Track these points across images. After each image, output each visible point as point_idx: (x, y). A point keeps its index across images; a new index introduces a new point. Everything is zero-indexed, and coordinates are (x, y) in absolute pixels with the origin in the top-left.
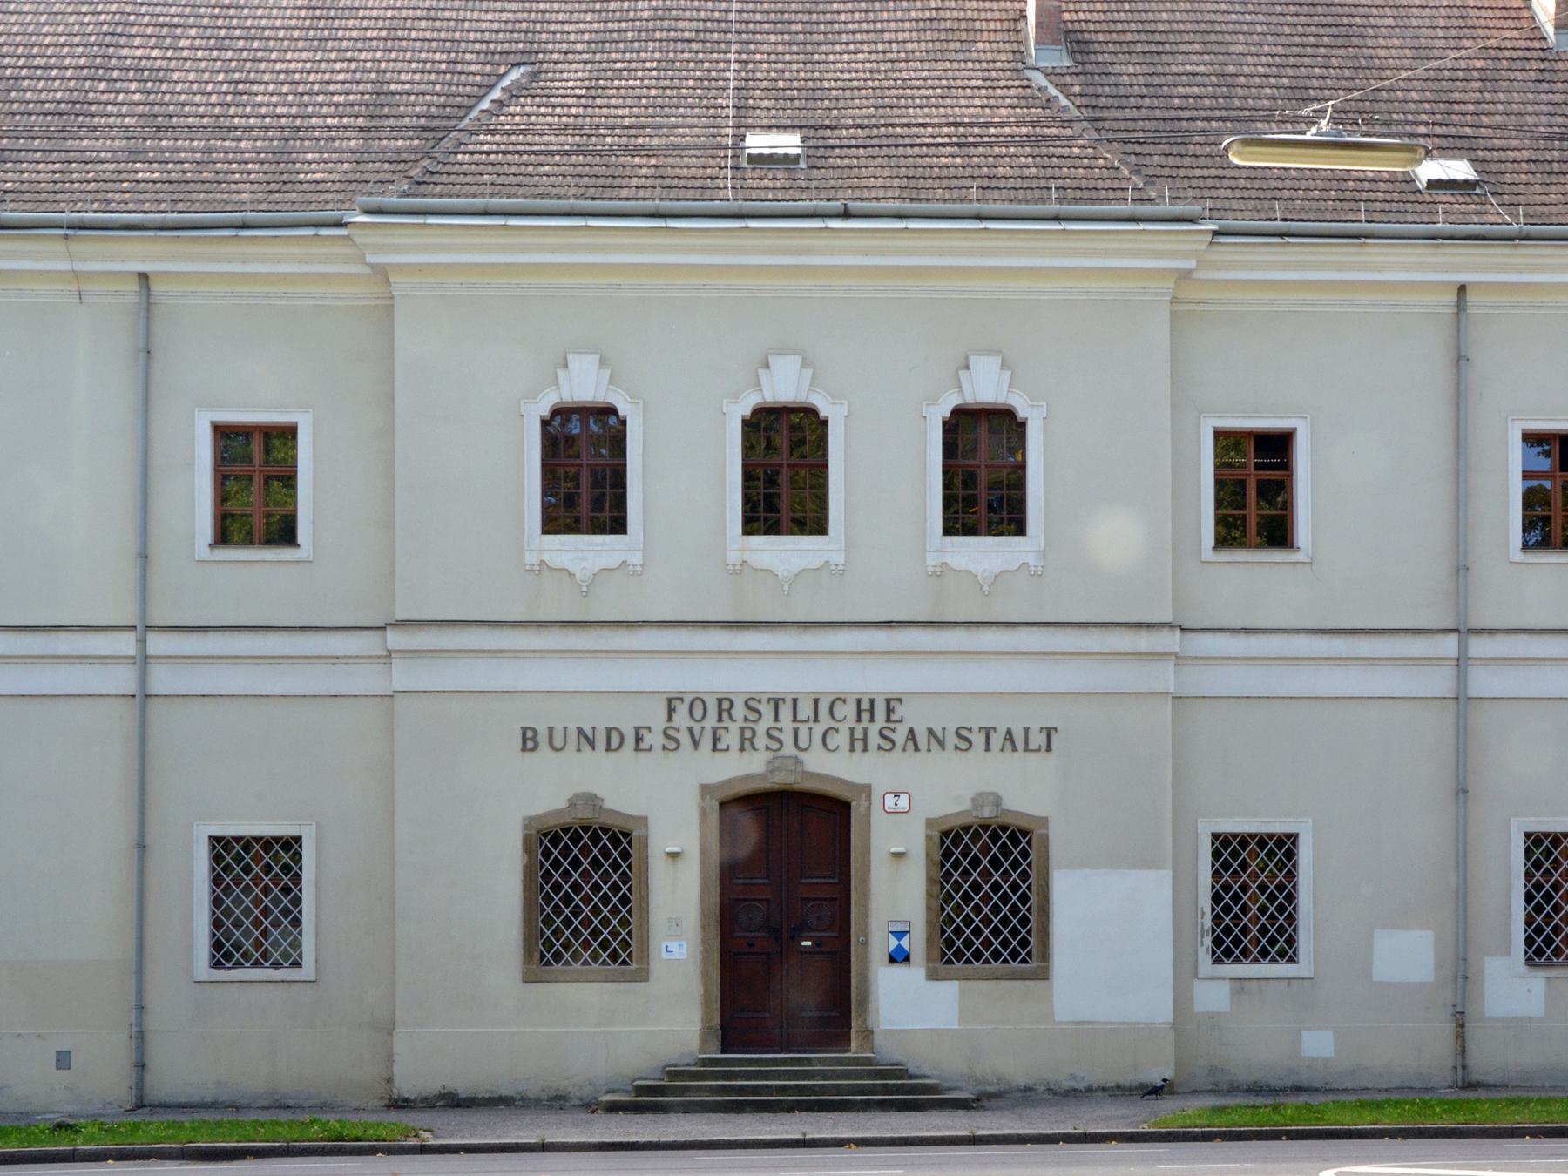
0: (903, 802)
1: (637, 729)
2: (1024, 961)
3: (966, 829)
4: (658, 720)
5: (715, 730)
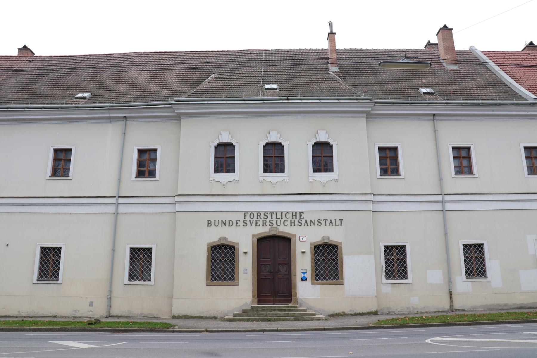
0: (304, 239)
1: (237, 221)
2: (337, 280)
3: (321, 245)
4: (242, 218)
5: (256, 221)
